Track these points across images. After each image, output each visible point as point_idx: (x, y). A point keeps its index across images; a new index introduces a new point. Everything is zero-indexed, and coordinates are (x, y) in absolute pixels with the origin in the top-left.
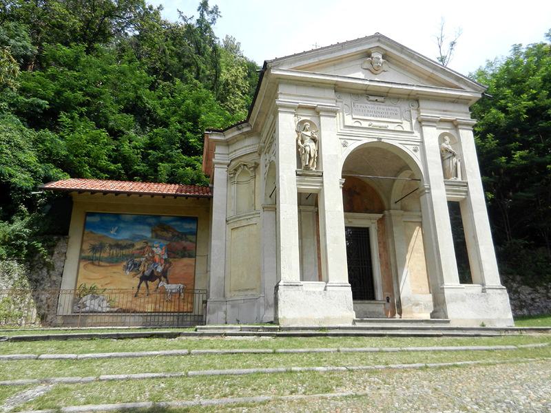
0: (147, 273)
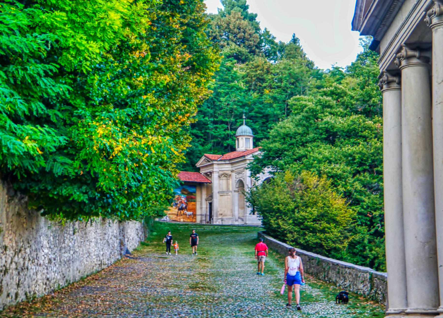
0: (180, 207)
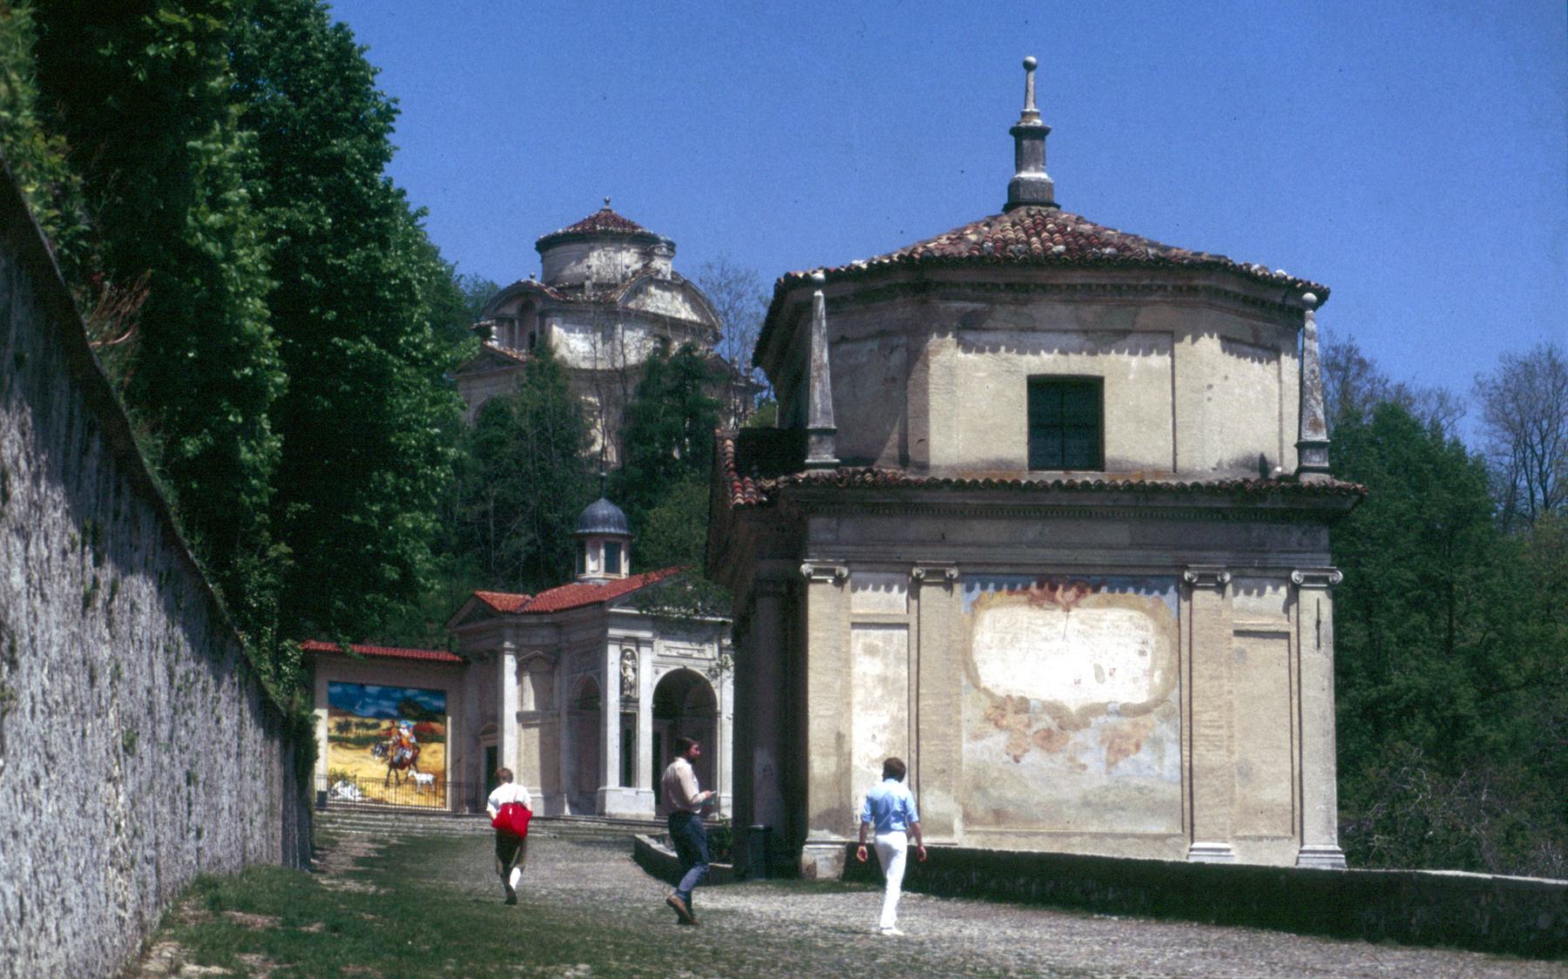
0: (396, 758)
